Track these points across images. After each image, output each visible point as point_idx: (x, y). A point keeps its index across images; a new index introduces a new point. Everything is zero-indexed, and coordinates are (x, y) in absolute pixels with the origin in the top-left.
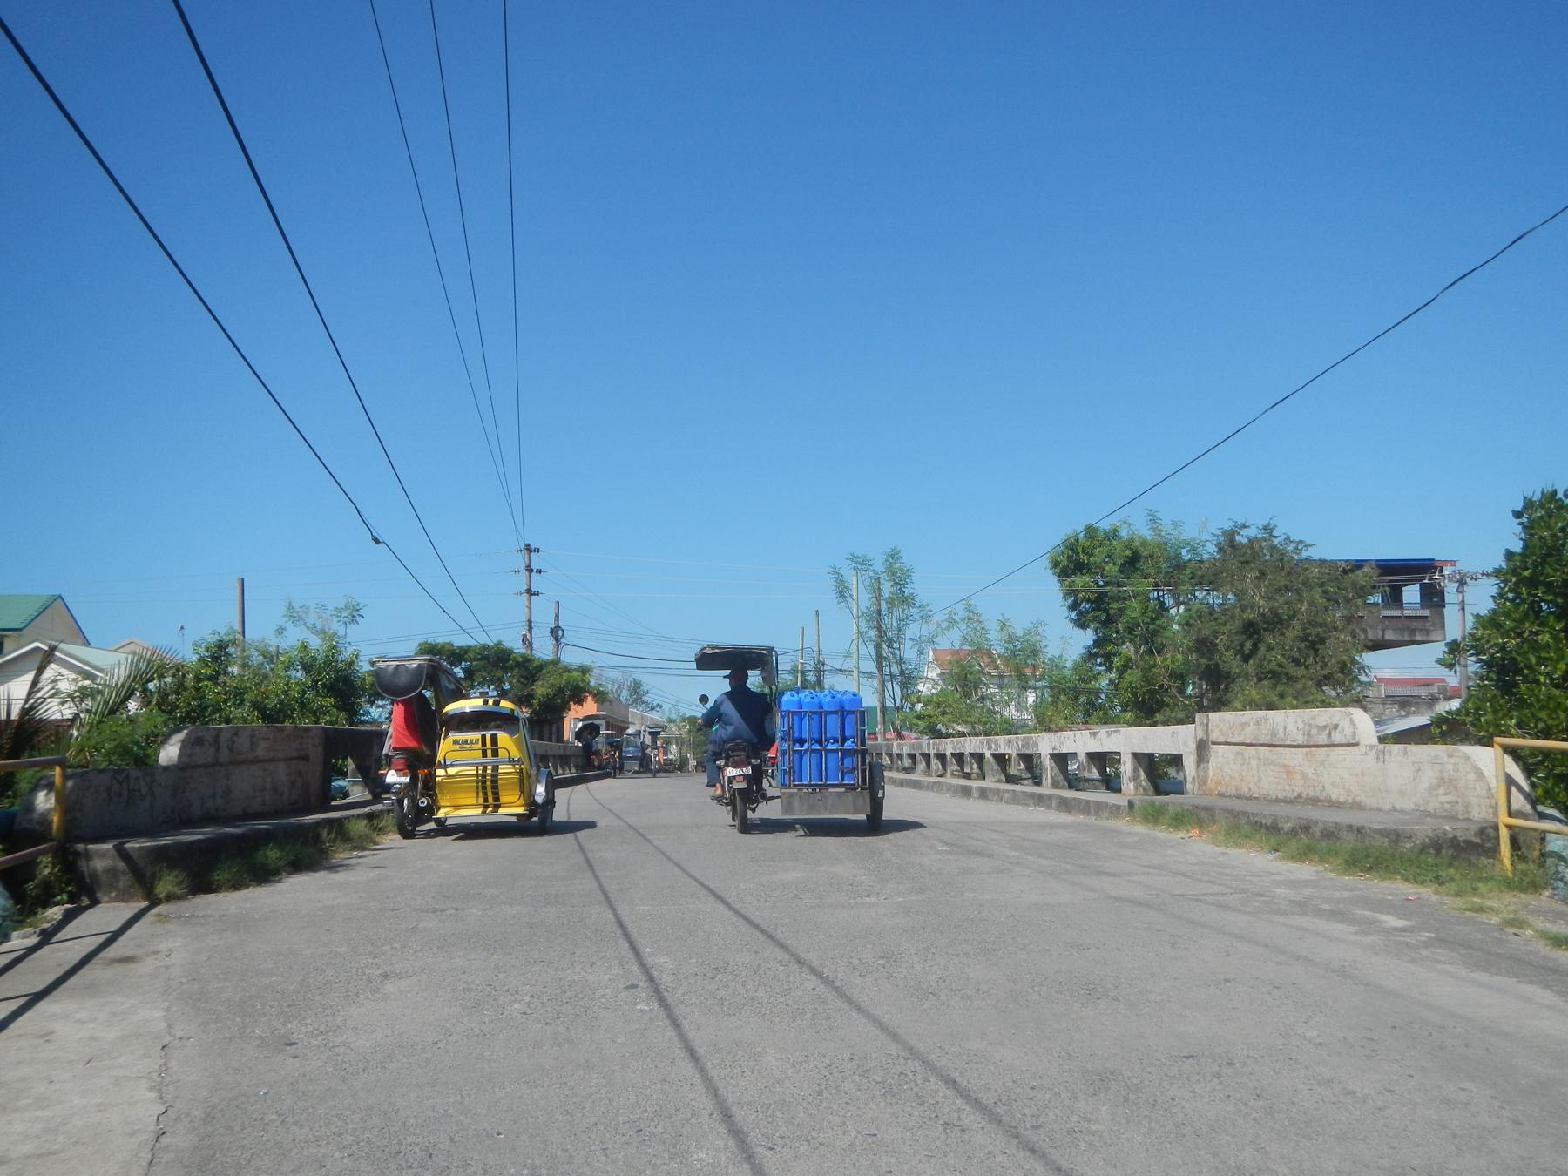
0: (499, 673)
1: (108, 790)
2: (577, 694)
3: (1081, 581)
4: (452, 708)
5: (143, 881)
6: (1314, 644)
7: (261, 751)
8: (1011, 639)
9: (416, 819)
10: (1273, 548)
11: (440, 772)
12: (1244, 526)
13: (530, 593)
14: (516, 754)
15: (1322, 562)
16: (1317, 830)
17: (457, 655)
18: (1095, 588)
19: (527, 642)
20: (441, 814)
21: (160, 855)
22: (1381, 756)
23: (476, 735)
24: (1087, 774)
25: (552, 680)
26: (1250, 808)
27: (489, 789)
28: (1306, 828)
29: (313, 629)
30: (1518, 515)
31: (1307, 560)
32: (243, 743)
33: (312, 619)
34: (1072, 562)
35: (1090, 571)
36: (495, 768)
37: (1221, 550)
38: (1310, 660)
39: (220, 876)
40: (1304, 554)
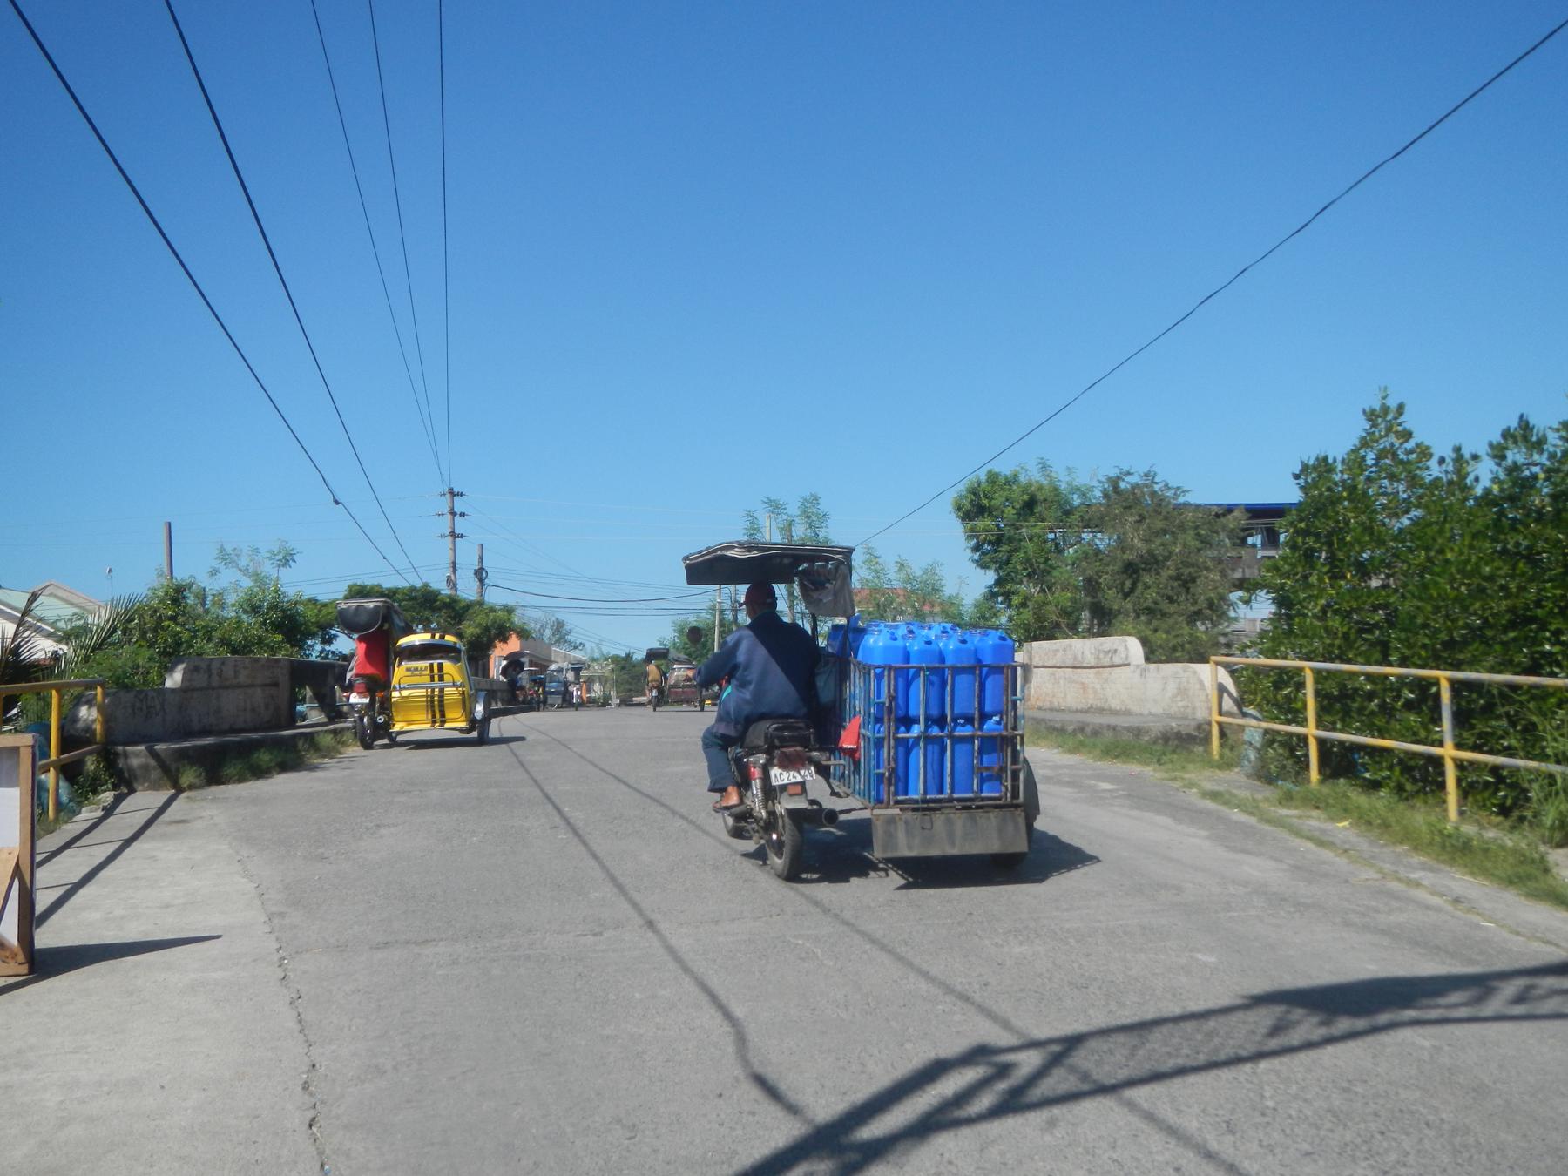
0: (427, 613)
1: (133, 706)
2: (502, 633)
3: (984, 523)
4: (405, 641)
5: (169, 775)
6: (1186, 583)
7: (242, 679)
8: (909, 580)
9: (377, 733)
10: (1153, 494)
11: (395, 694)
12: (1129, 473)
14: (459, 680)
15: (1198, 506)
16: (1088, 730)
18: (996, 531)
20: (397, 728)
21: (183, 755)
22: (1143, 672)
23: (425, 664)
25: (478, 620)
26: (1048, 716)
27: (437, 708)
28: (1081, 729)
30: (1297, 477)
31: (1186, 505)
32: (229, 671)
33: (244, 561)
34: (974, 507)
36: (442, 691)
37: (1106, 496)
38: (1182, 598)
39: (230, 770)
40: (1181, 500)
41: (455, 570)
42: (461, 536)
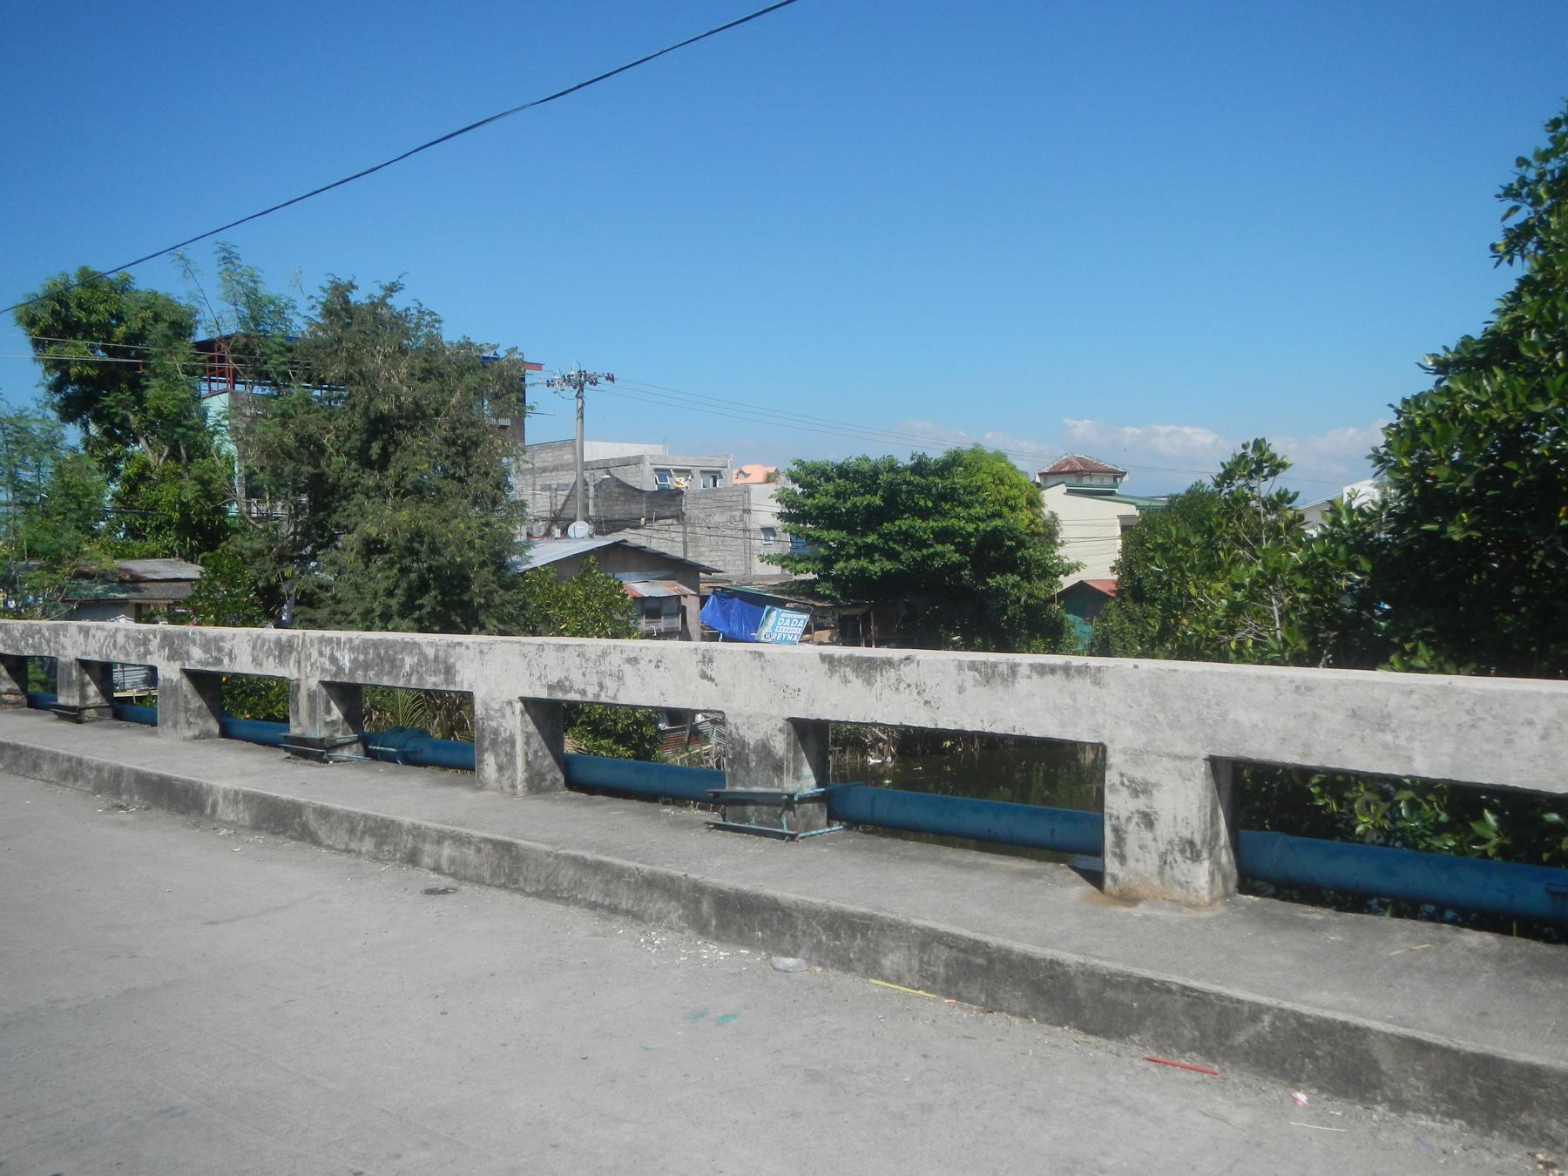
6: (464, 447)
24: (789, 785)
34: (58, 320)
35: (88, 335)
37: (329, 312)
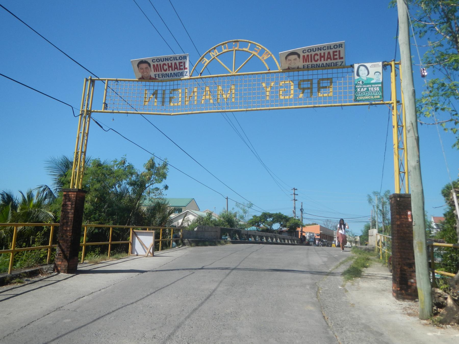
5: (190, 244)
13: (295, 200)
17: (270, 216)
19: (294, 213)
21: (192, 241)
25: (291, 222)
29: (241, 208)
33: (241, 206)
41: (295, 209)
42: (296, 200)
